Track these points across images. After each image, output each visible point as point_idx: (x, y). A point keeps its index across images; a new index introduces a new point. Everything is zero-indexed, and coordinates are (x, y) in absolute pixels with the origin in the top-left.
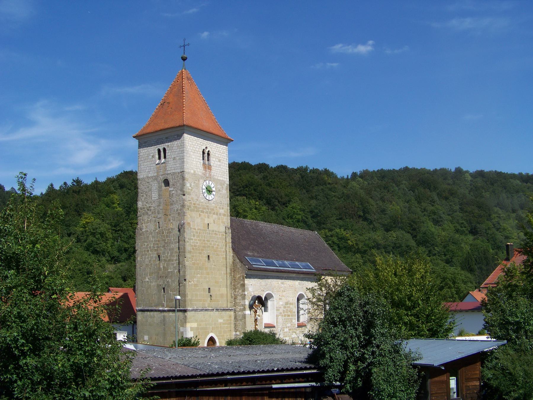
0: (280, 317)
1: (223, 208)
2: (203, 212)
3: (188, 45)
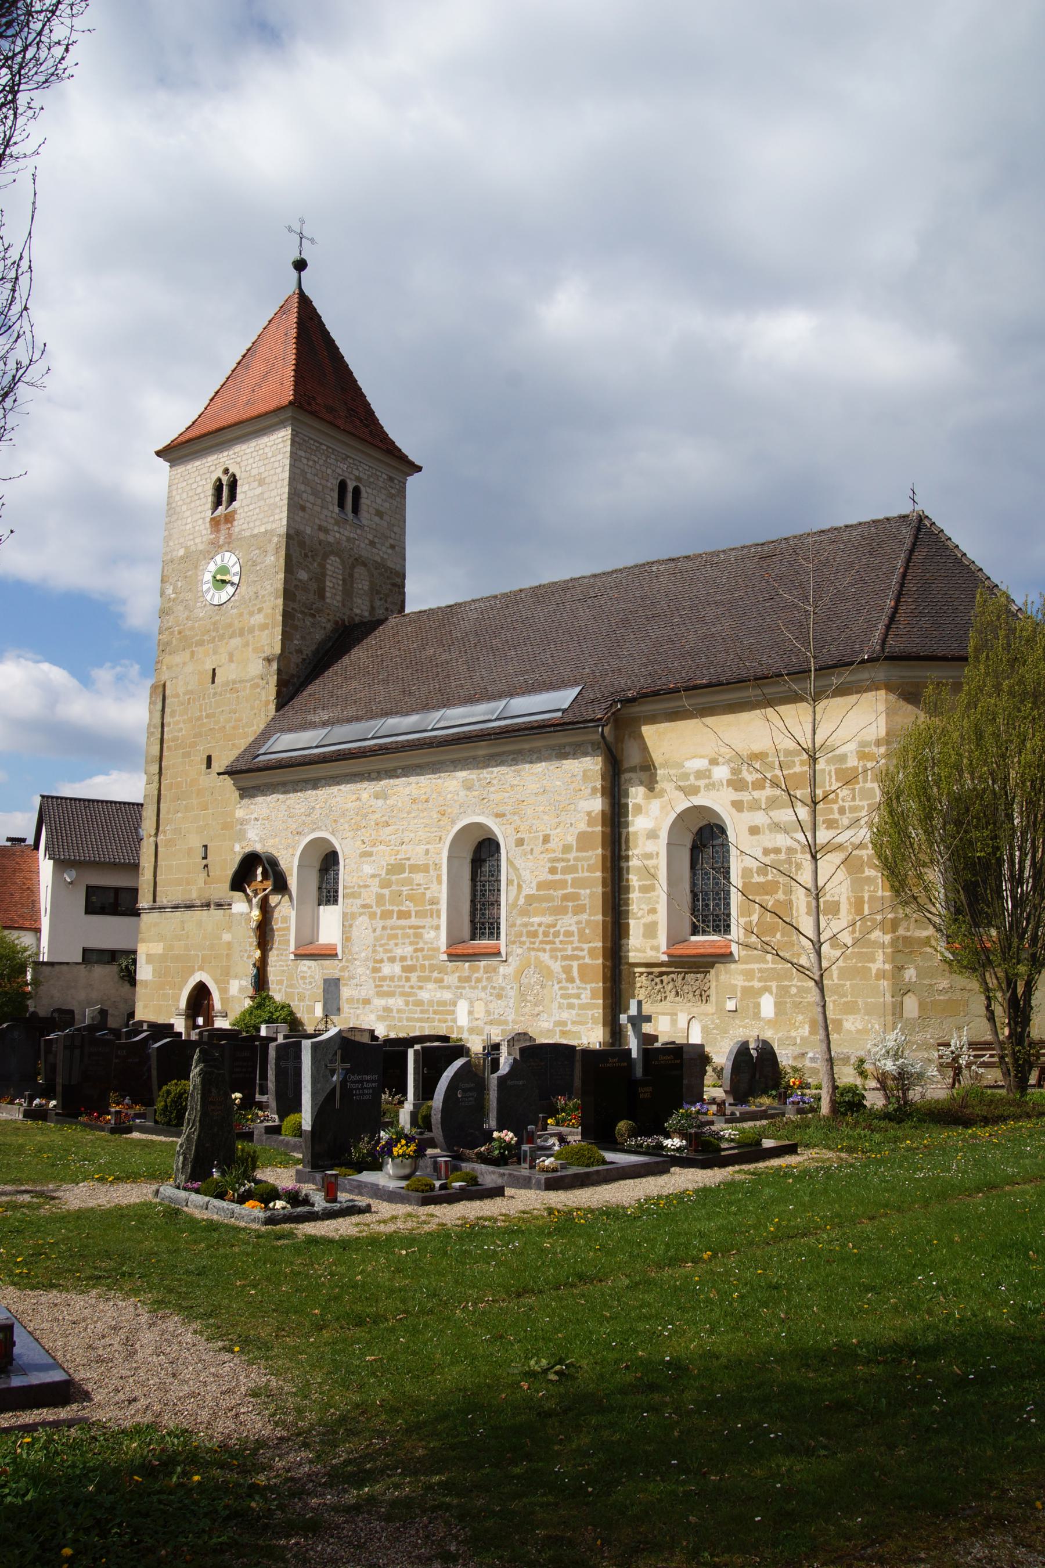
0: (363, 921)
1: (260, 610)
2: (200, 643)
3: (302, 222)
